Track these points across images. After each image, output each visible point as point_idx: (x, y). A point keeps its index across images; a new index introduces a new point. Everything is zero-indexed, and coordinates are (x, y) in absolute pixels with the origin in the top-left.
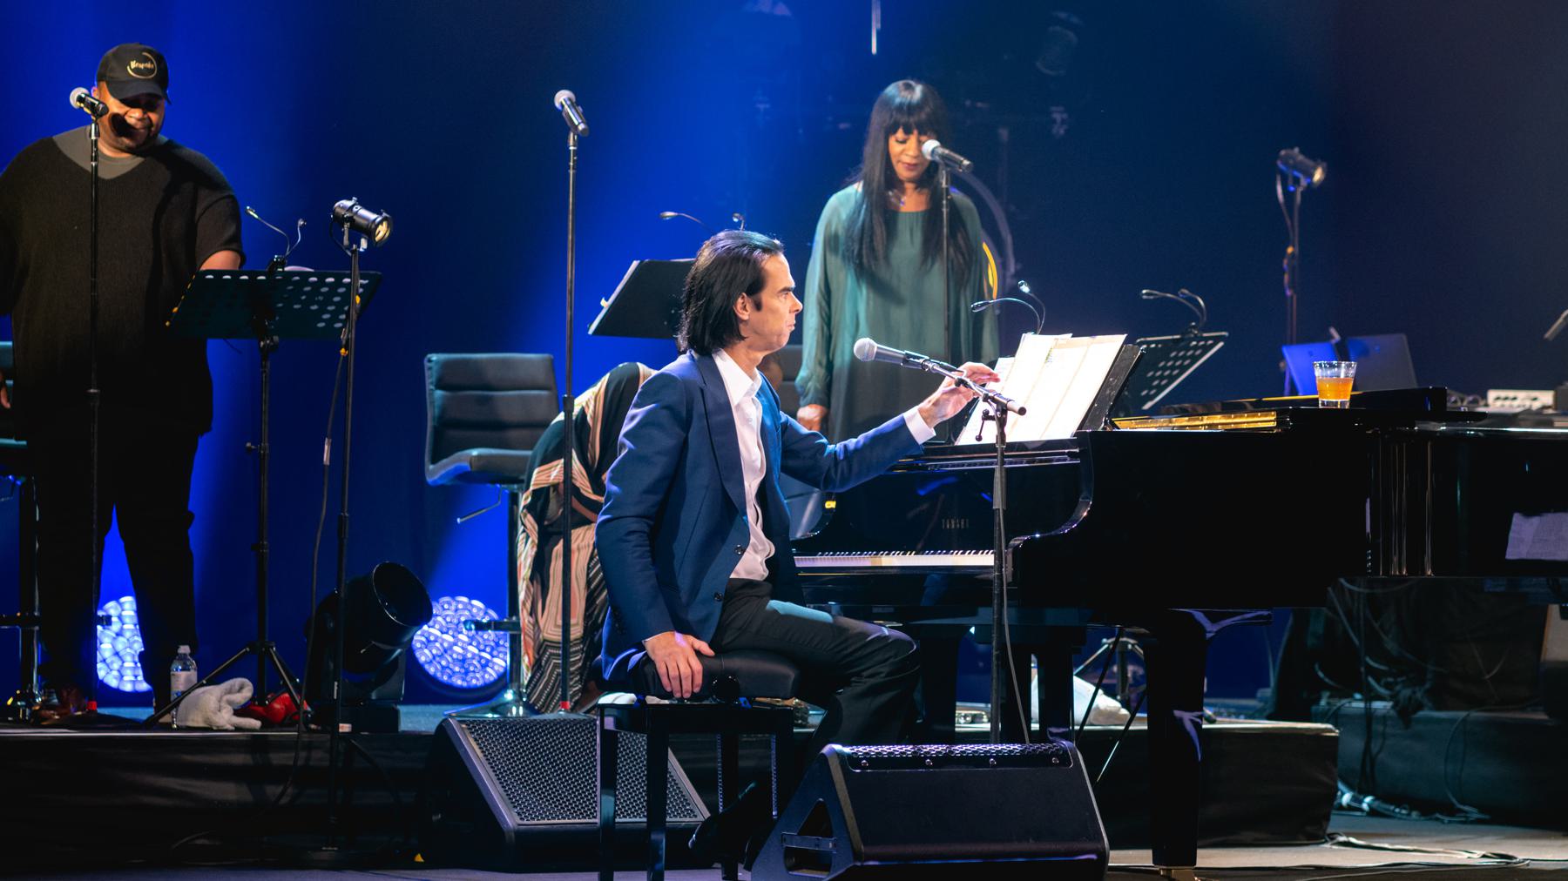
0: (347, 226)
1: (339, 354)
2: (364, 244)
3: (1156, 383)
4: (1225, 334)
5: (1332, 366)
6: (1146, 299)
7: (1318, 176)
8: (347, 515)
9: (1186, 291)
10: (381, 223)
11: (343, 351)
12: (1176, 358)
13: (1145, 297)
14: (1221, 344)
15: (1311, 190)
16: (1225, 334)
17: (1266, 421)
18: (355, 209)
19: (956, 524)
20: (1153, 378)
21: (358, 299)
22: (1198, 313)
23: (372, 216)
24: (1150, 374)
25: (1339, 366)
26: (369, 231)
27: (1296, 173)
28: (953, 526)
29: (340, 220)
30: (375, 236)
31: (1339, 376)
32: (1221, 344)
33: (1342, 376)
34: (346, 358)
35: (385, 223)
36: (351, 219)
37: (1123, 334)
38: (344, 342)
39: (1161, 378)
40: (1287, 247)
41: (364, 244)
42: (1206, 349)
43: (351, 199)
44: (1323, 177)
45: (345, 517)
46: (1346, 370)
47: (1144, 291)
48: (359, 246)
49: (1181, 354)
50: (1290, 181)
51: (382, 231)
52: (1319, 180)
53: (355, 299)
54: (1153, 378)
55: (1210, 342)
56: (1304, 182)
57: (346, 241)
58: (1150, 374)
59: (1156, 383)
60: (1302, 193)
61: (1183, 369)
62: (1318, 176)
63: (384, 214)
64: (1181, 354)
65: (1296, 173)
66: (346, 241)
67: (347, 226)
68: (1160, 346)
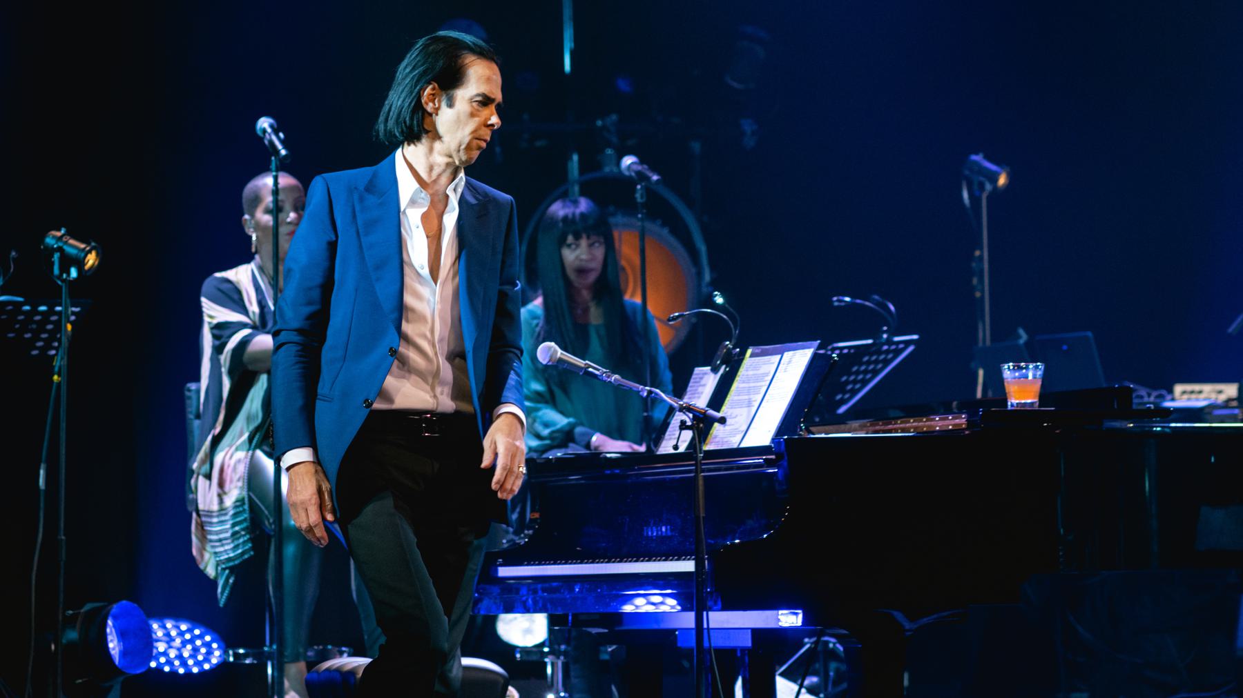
0: (56, 256)
1: (52, 381)
2: (74, 273)
3: (850, 387)
4: (915, 337)
5: (1020, 368)
6: (838, 306)
7: (1002, 181)
8: (63, 538)
9: (876, 297)
10: (90, 252)
11: (56, 377)
12: (869, 363)
13: (836, 304)
14: (911, 348)
15: (996, 194)
16: (915, 337)
17: (955, 421)
18: (64, 239)
19: (657, 531)
20: (847, 382)
21: (69, 327)
22: (889, 319)
23: (83, 246)
24: (844, 378)
25: (1027, 368)
26: (80, 263)
27: (982, 179)
28: (655, 534)
29: (52, 251)
30: (85, 265)
31: (1027, 377)
32: (911, 348)
33: (1030, 377)
34: (59, 384)
35: (94, 253)
36: (60, 249)
37: (816, 340)
38: (56, 369)
39: (855, 382)
40: (974, 250)
41: (74, 273)
42: (898, 352)
43: (59, 230)
44: (1005, 182)
45: (61, 539)
46: (1034, 372)
47: (835, 299)
48: (69, 274)
49: (874, 358)
50: (976, 187)
51: (91, 260)
52: (1003, 185)
53: (66, 327)
54: (847, 382)
55: (901, 346)
56: (988, 187)
57: (56, 271)
58: (844, 378)
59: (850, 387)
60: (988, 198)
61: (875, 373)
62: (1002, 181)
63: (93, 244)
64: (874, 358)
65: (982, 179)
66: (56, 271)
67: (56, 256)
68: (852, 351)
